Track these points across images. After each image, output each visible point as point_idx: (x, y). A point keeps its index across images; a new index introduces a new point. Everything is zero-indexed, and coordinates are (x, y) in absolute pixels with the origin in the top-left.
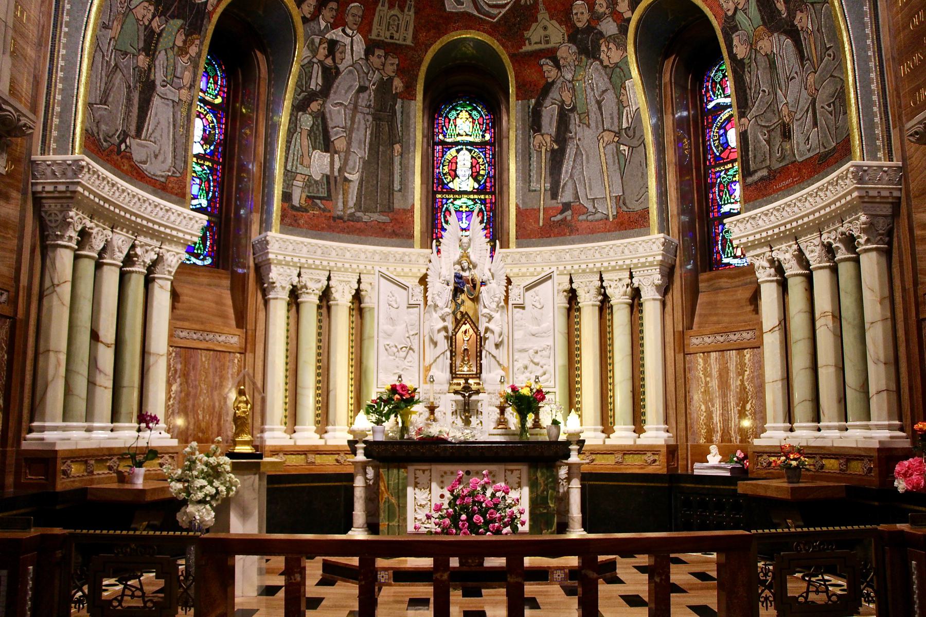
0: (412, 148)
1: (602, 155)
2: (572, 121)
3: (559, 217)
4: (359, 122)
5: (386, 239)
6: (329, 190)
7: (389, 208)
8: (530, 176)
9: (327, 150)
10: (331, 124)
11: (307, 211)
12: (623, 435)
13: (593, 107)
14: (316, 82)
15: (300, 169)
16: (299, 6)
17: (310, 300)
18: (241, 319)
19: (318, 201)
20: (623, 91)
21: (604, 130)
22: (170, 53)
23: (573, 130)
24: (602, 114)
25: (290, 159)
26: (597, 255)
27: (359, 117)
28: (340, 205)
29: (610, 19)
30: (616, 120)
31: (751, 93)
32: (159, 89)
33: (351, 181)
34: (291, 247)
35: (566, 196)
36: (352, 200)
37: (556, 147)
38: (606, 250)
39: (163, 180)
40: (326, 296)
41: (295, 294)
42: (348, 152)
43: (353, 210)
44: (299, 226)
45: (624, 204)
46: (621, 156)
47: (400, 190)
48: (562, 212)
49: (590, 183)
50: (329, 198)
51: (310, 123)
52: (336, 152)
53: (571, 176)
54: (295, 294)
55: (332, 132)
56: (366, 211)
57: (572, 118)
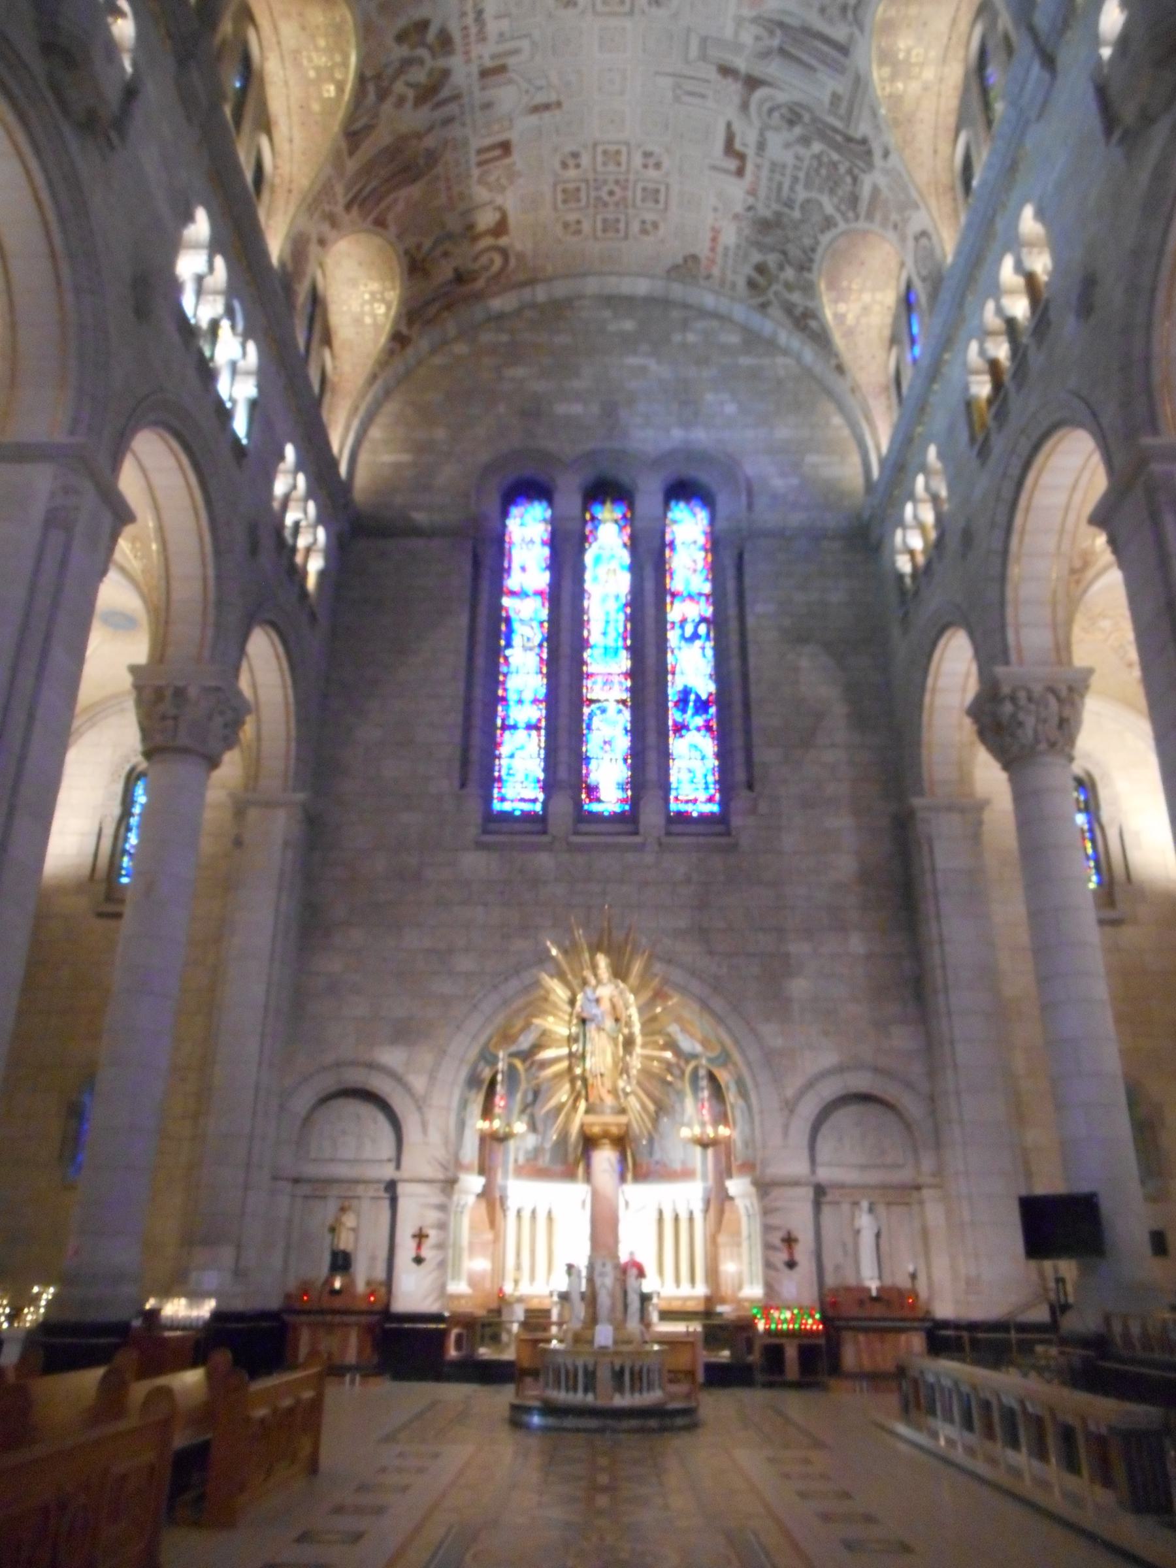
12: (685, 1290)
14: (530, 1097)
17: (526, 1215)
18: (492, 1223)
40: (534, 1212)
41: (519, 1212)
54: (519, 1212)
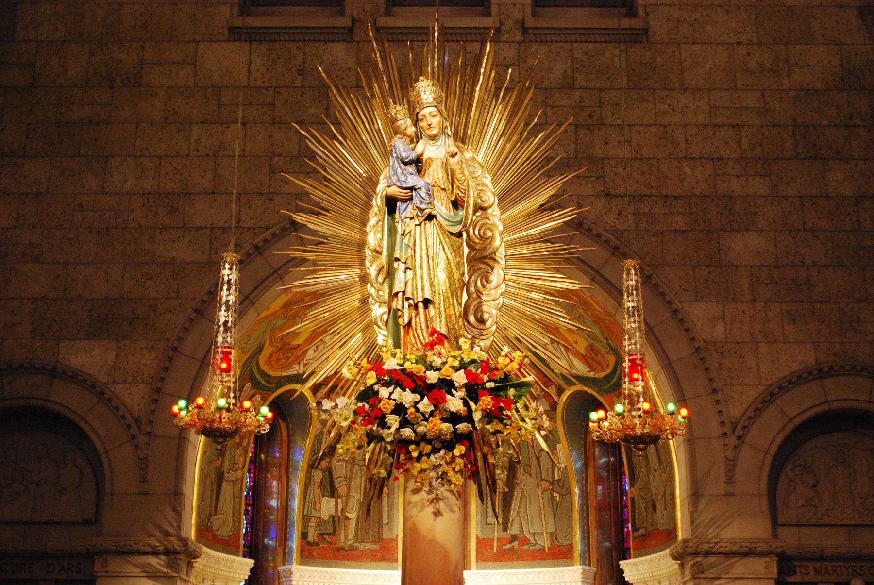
0: (396, 490)
1: (541, 498)
2: (518, 470)
3: (509, 546)
4: (357, 472)
5: (377, 564)
6: (334, 528)
7: (379, 538)
8: (487, 512)
9: (332, 495)
10: (335, 476)
11: (318, 545)
13: (534, 462)
15: (314, 513)
16: (314, 395)
19: (326, 537)
20: (555, 451)
21: (542, 480)
22: (233, 449)
23: (519, 478)
24: (540, 467)
25: (306, 506)
26: (536, 578)
27: (356, 468)
28: (342, 538)
29: (544, 399)
30: (550, 473)
31: (636, 471)
32: (226, 476)
33: (350, 519)
34: (307, 575)
35: (514, 530)
36: (351, 533)
37: (506, 490)
38: (542, 575)
39: (227, 538)
42: (348, 496)
43: (352, 542)
44: (313, 557)
45: (556, 539)
46: (554, 501)
47: (387, 524)
48: (511, 542)
49: (532, 521)
50: (334, 533)
51: (320, 477)
52: (339, 497)
53: (518, 514)
55: (336, 481)
56: (362, 541)
57: (518, 468)
